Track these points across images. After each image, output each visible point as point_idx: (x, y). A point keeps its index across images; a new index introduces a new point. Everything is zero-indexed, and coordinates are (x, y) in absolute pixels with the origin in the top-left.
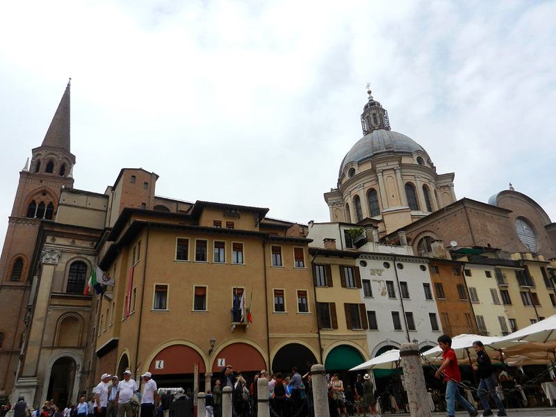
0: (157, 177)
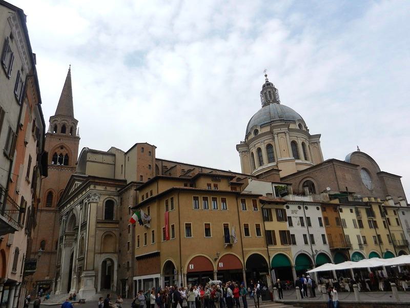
0: (156, 147)
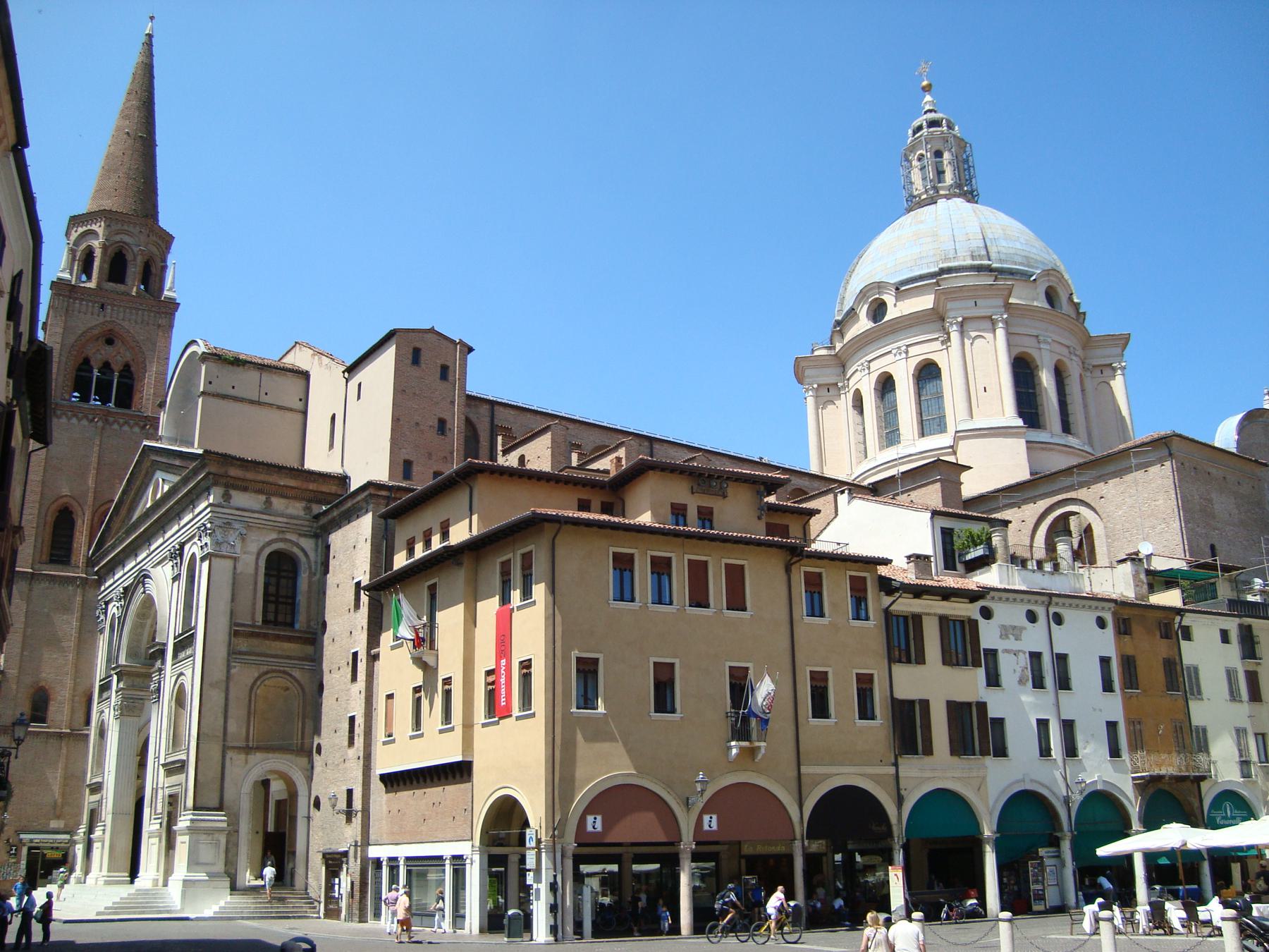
0: (471, 350)
